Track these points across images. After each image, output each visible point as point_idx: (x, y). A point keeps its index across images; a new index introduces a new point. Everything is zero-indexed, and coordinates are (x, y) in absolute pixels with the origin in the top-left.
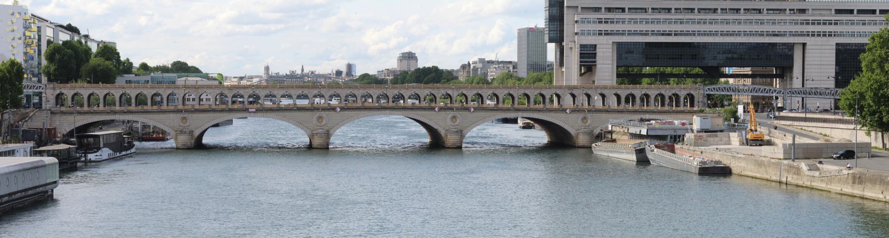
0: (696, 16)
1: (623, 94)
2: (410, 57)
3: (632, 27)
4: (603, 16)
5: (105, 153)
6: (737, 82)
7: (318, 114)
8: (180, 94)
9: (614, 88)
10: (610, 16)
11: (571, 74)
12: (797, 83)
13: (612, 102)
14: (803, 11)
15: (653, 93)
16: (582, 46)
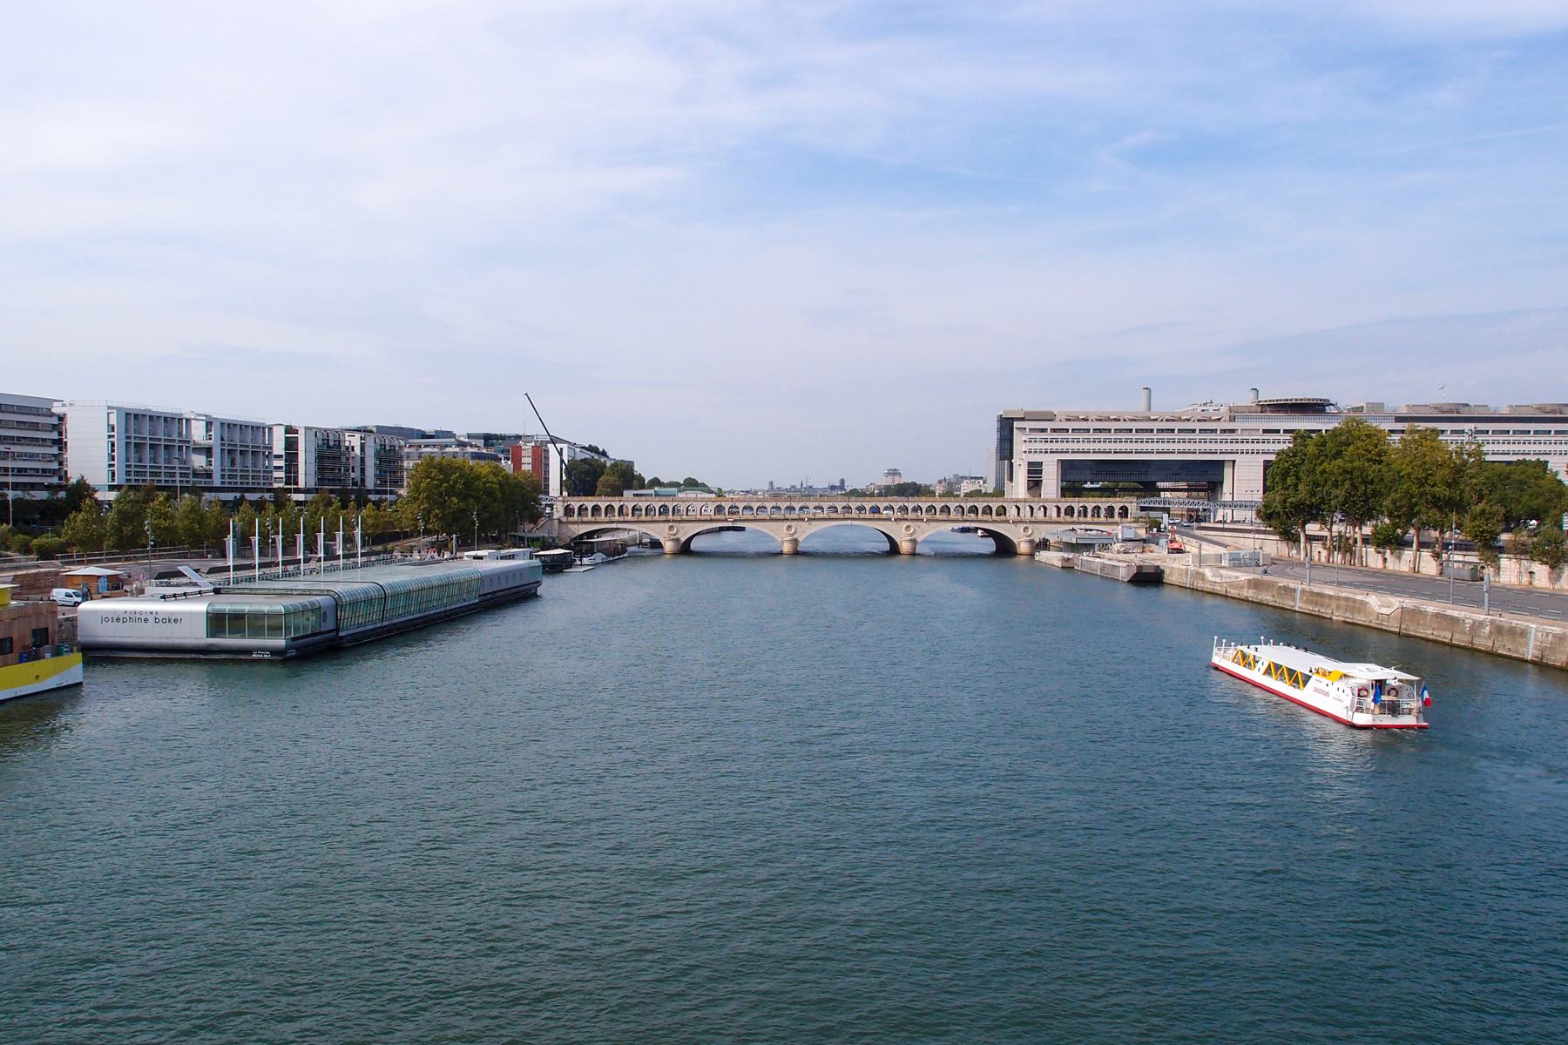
1: (1063, 507)
2: (894, 473)
3: (1075, 446)
4: (1048, 436)
5: (599, 557)
6: (1175, 497)
7: (786, 524)
8: (683, 508)
9: (1052, 501)
10: (1055, 435)
11: (1019, 487)
12: (1227, 497)
13: (1053, 512)
14: (1233, 431)
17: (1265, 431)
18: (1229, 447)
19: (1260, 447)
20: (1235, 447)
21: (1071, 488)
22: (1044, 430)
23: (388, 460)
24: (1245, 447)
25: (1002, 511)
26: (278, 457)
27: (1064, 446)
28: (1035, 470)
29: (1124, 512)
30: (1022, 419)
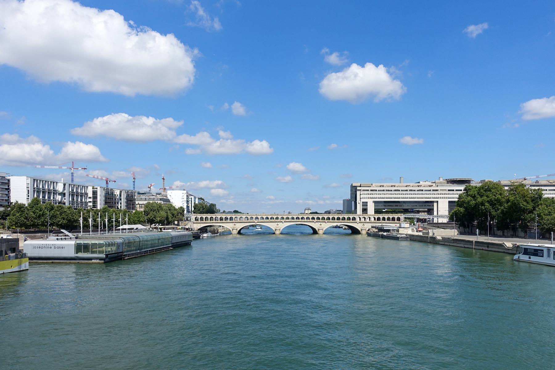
0: (401, 192)
1: (376, 217)
3: (379, 196)
4: (370, 192)
10: (372, 192)
12: (435, 213)
13: (372, 219)
14: (437, 190)
15: (386, 217)
16: (363, 202)
17: (449, 190)
18: (436, 196)
19: (447, 196)
20: (438, 196)
21: (377, 211)
22: (368, 190)
23: (130, 200)
24: (441, 196)
25: (354, 219)
26: (90, 198)
27: (375, 196)
28: (365, 204)
29: (399, 219)
30: (360, 186)
